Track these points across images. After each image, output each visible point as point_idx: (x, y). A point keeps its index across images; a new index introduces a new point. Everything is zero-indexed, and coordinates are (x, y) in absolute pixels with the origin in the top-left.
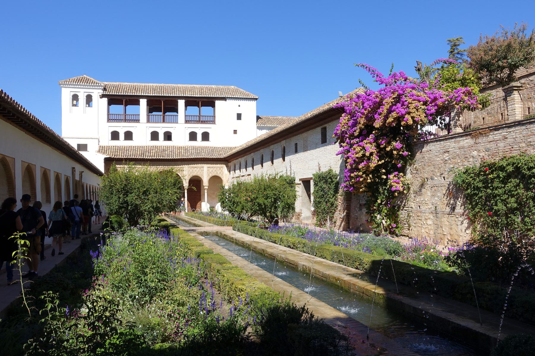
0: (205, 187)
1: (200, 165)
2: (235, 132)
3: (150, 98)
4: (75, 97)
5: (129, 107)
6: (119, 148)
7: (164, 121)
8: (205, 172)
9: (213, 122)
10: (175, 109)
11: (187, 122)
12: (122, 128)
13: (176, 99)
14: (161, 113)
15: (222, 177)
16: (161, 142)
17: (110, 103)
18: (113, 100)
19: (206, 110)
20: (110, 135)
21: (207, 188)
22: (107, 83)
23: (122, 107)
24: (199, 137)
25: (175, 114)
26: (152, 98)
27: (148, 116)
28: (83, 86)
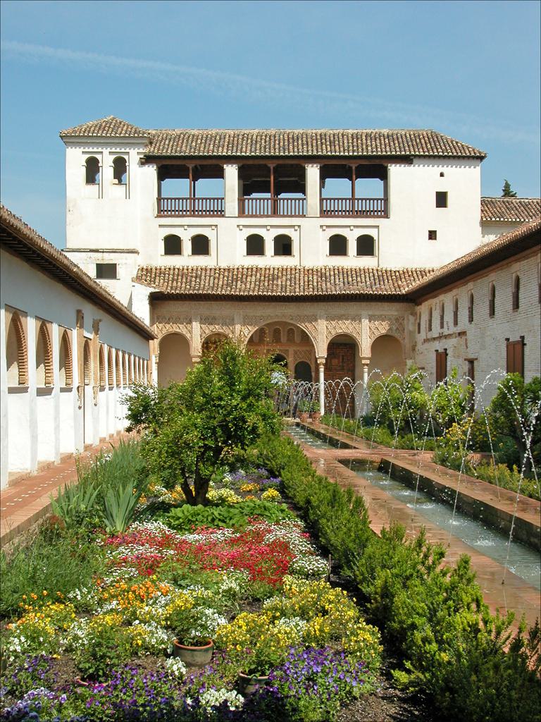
2: (432, 235)
5: (201, 183)
6: (181, 273)
7: (275, 213)
9: (385, 213)
10: (300, 187)
11: (324, 213)
13: (301, 162)
14: (268, 195)
16: (269, 259)
17: (163, 174)
18: (169, 168)
19: (368, 187)
20: (162, 243)
23: (186, 183)
25: (300, 195)
26: (251, 162)
27: (241, 202)
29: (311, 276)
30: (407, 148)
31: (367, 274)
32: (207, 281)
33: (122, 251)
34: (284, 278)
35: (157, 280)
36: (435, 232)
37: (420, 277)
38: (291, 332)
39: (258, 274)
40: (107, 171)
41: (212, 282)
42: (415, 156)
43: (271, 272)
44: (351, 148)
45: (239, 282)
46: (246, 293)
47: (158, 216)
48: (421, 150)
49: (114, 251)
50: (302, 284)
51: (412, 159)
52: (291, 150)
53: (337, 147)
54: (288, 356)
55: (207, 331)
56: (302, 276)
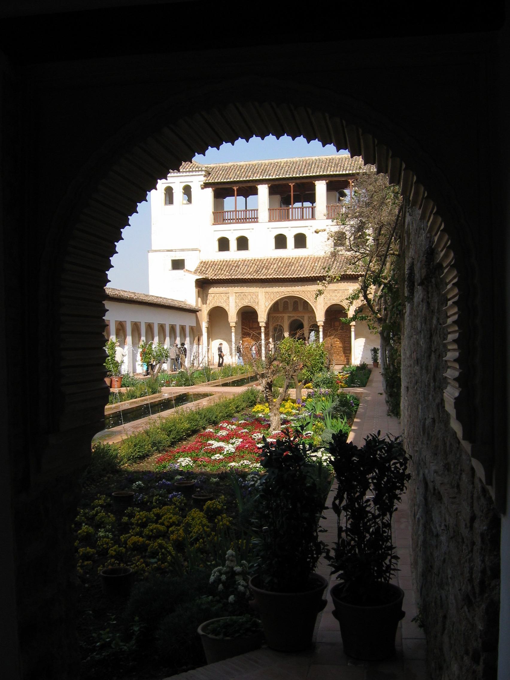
5: (251, 198)
6: (228, 264)
12: (232, 232)
13: (313, 180)
16: (291, 251)
18: (222, 191)
20: (217, 244)
22: (214, 165)
29: (317, 262)
33: (188, 250)
34: (297, 265)
39: (280, 263)
40: (178, 194)
43: (290, 261)
44: (348, 168)
45: (264, 269)
46: (264, 277)
47: (213, 224)
49: (183, 250)
52: (305, 172)
53: (339, 168)
54: (304, 320)
55: (240, 305)
56: (311, 262)
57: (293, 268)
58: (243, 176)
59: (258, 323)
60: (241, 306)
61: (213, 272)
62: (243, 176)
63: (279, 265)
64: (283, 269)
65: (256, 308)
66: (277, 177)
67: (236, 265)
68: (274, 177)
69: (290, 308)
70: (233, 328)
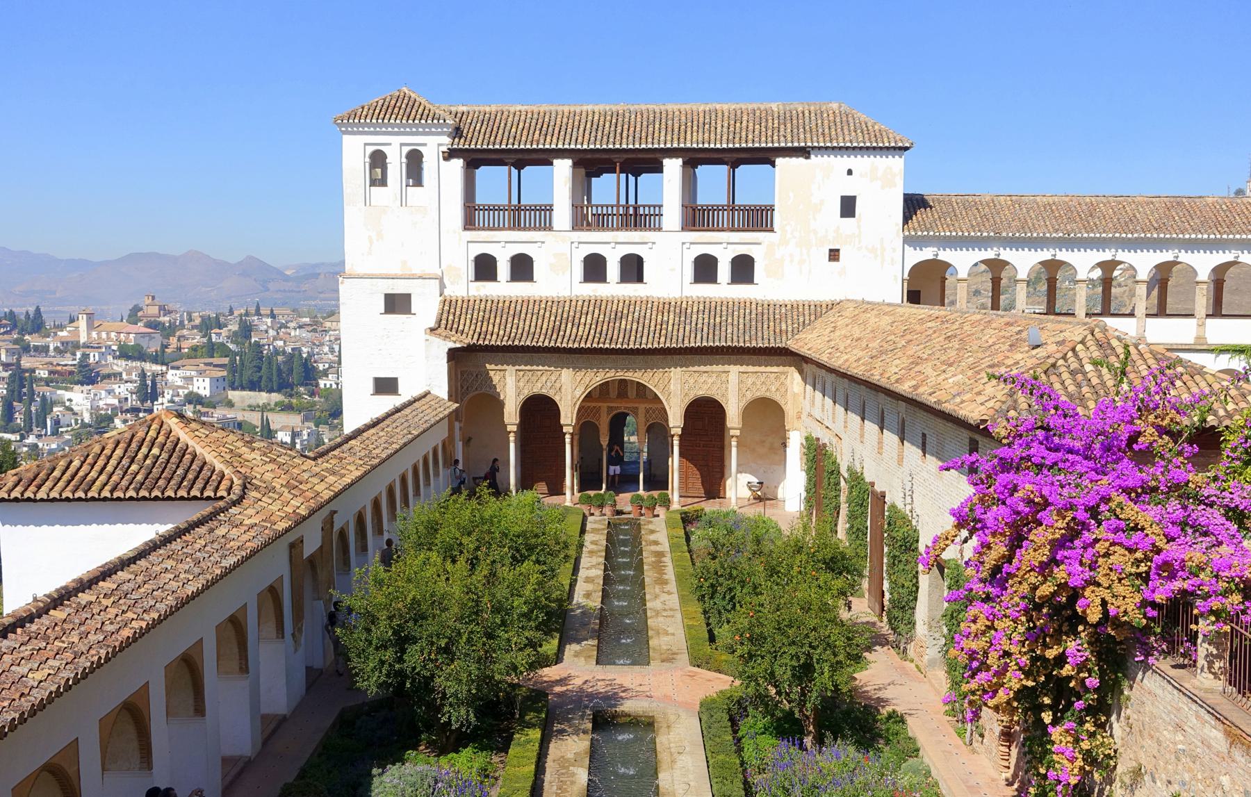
0: (732, 432)
1: (720, 368)
2: (834, 255)
3: (582, 156)
4: (378, 160)
6: (496, 308)
8: (733, 387)
12: (503, 246)
13: (658, 155)
15: (782, 403)
16: (613, 288)
21: (737, 433)
22: (465, 109)
24: (724, 271)
26: (589, 156)
28: (398, 126)
30: (802, 136)
31: (742, 311)
32: (528, 323)
34: (630, 318)
35: (462, 321)
36: (838, 250)
37: (813, 318)
38: (641, 389)
39: (597, 311)
41: (533, 324)
42: (813, 148)
44: (725, 137)
45: (570, 325)
46: (576, 345)
47: (465, 229)
48: (821, 139)
50: (652, 329)
51: (809, 153)
56: (654, 313)
57: (623, 326)
58: (524, 138)
59: (561, 427)
60: (527, 392)
61: (473, 327)
62: (524, 138)
63: (596, 315)
64: (605, 327)
65: (557, 399)
66: (592, 146)
67: (512, 312)
68: (585, 147)
69: (613, 393)
70: (512, 434)
